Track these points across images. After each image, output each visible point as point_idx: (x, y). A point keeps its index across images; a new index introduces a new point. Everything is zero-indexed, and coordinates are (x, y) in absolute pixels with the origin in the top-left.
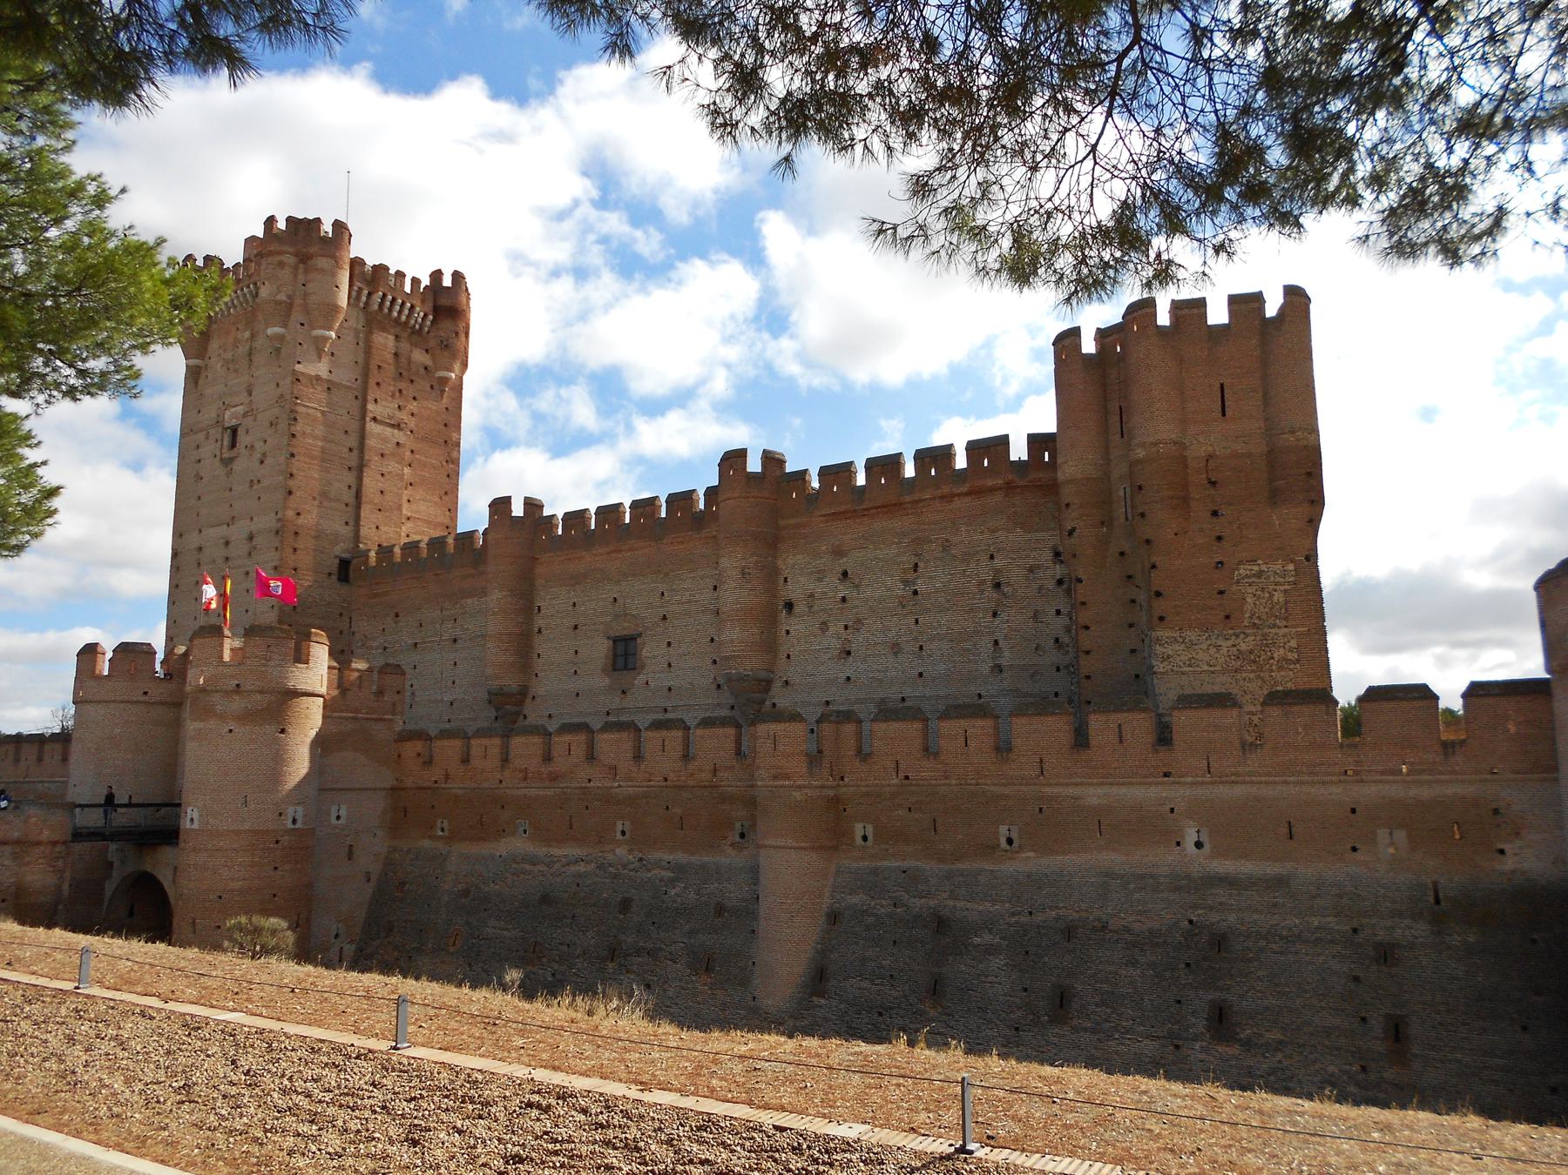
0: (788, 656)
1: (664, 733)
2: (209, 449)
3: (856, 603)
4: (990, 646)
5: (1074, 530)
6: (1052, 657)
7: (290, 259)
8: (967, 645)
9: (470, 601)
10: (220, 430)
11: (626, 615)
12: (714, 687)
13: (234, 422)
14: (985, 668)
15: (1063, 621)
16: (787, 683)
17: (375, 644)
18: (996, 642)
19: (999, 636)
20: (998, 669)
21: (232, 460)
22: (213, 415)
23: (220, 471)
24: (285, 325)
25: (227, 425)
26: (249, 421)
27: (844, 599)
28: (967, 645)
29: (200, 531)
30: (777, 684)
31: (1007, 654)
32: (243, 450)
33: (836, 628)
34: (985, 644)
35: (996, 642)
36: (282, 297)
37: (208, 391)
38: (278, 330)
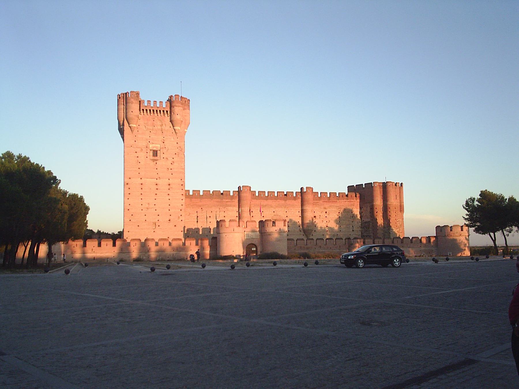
0: (315, 226)
1: (330, 241)
2: (142, 155)
3: (329, 218)
4: (352, 227)
5: (377, 212)
6: (360, 229)
7: (182, 108)
8: (348, 226)
9: (229, 208)
10: (149, 150)
11: (277, 215)
12: (299, 231)
13: (155, 149)
14: (351, 230)
15: (360, 223)
16: (315, 231)
17: (193, 215)
18: (353, 226)
19: (353, 225)
20: (353, 231)
21: (157, 160)
22: (144, 144)
23: (152, 164)
24: (180, 127)
25: (150, 149)
26: (164, 150)
27: (326, 217)
28: (348, 226)
29: (141, 179)
30: (313, 231)
31: (355, 228)
32: (162, 158)
33: (325, 222)
34: (351, 226)
35: (353, 226)
36: (182, 120)
37: (140, 136)
38: (179, 128)
